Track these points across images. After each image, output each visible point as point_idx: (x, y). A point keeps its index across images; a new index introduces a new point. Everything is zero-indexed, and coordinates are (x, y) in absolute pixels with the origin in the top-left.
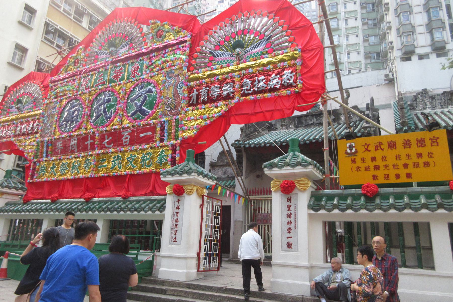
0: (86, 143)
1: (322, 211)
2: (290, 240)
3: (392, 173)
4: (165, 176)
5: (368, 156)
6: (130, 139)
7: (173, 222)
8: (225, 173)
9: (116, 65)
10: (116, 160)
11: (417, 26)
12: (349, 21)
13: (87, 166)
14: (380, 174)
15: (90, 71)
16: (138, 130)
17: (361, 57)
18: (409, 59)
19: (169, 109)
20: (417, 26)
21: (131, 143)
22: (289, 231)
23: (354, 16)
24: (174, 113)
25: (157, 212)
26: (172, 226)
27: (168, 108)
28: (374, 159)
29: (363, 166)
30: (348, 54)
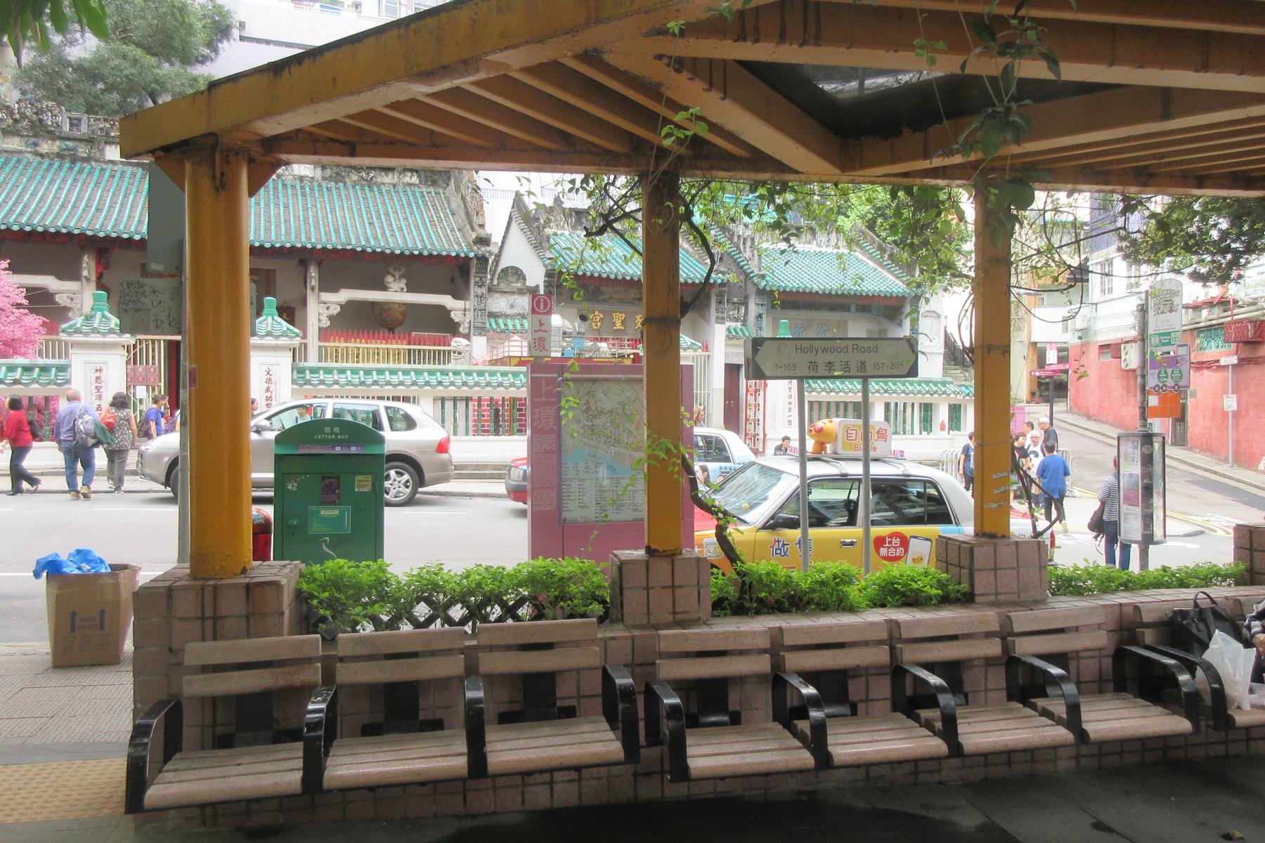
8: (512, 306)
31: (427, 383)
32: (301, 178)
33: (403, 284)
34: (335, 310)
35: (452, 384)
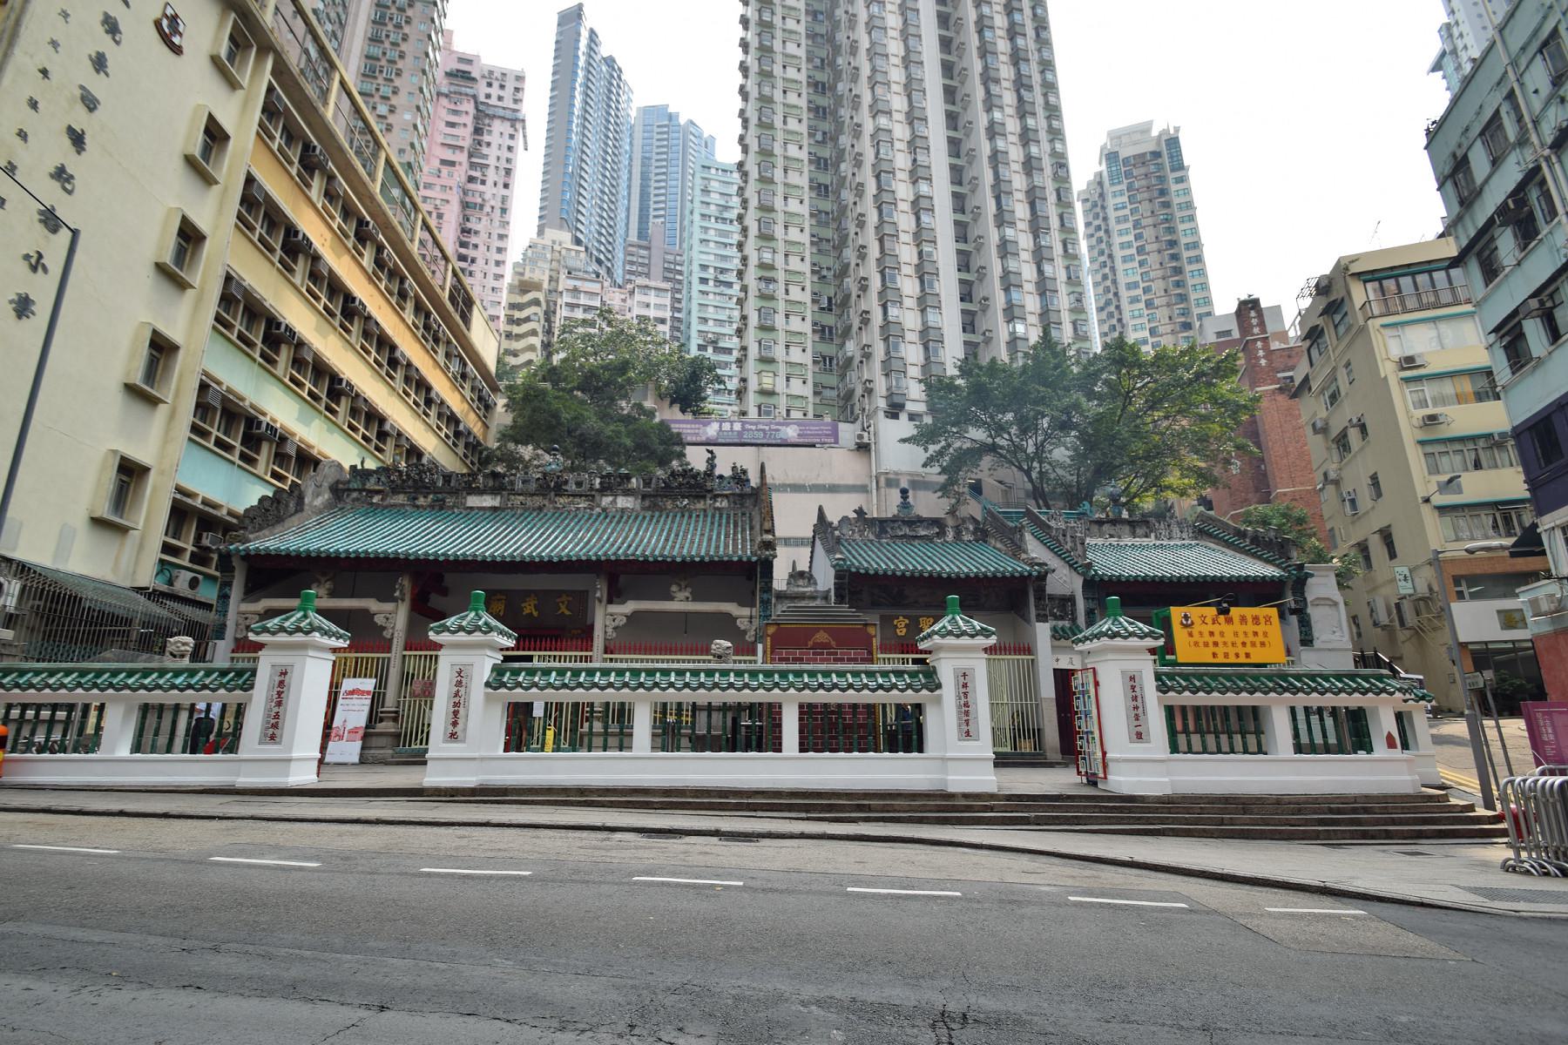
1: (1171, 694)
2: (1139, 729)
3: (1232, 651)
4: (943, 636)
5: (1206, 629)
7: (959, 707)
14: (1220, 650)
17: (808, 391)
18: (895, 416)
22: (1137, 717)
25: (924, 692)
26: (959, 713)
28: (1212, 634)
29: (1201, 641)
30: (788, 379)
32: (623, 510)
33: (687, 594)
34: (622, 621)
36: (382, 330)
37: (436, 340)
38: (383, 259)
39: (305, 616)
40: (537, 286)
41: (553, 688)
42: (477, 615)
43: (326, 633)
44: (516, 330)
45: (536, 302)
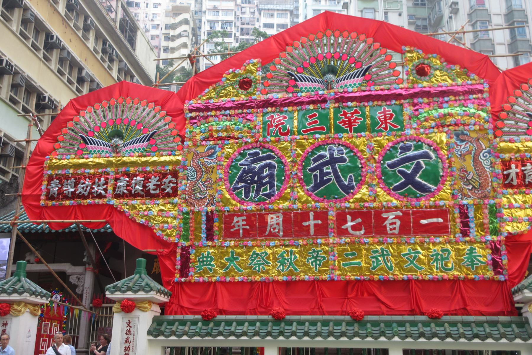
0: (305, 224)
6: (401, 225)
9: (344, 104)
10: (380, 256)
11: (497, 44)
12: (390, 15)
13: (315, 261)
15: (288, 105)
16: (414, 213)
19: (470, 187)
20: (497, 44)
21: (405, 230)
23: (398, 9)
24: (479, 194)
25: (518, 341)
27: (467, 185)
31: (269, 334)
35: (294, 334)
36: (73, 57)
37: (111, 60)
38: (72, 5)
39: (19, 280)
40: (186, 9)
41: (199, 335)
42: (140, 277)
43: (34, 293)
44: (171, 45)
45: (186, 22)
